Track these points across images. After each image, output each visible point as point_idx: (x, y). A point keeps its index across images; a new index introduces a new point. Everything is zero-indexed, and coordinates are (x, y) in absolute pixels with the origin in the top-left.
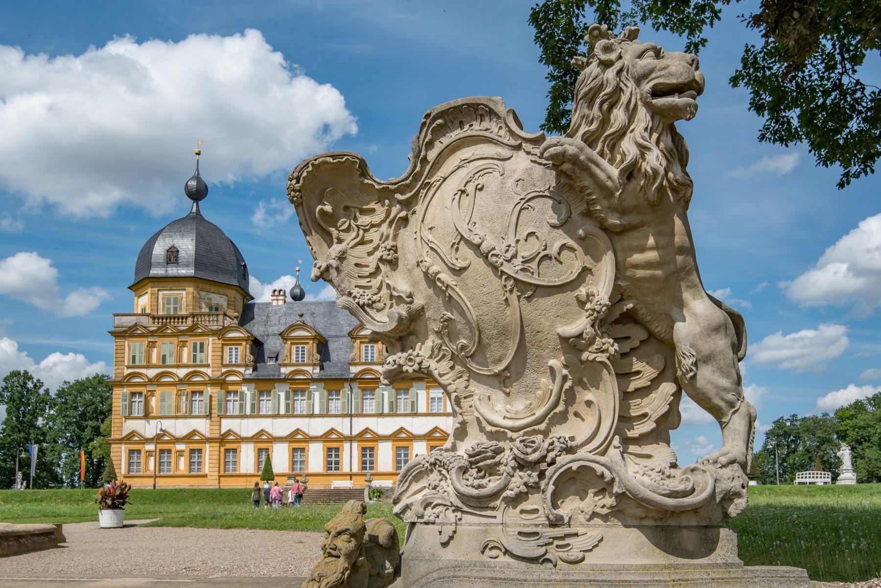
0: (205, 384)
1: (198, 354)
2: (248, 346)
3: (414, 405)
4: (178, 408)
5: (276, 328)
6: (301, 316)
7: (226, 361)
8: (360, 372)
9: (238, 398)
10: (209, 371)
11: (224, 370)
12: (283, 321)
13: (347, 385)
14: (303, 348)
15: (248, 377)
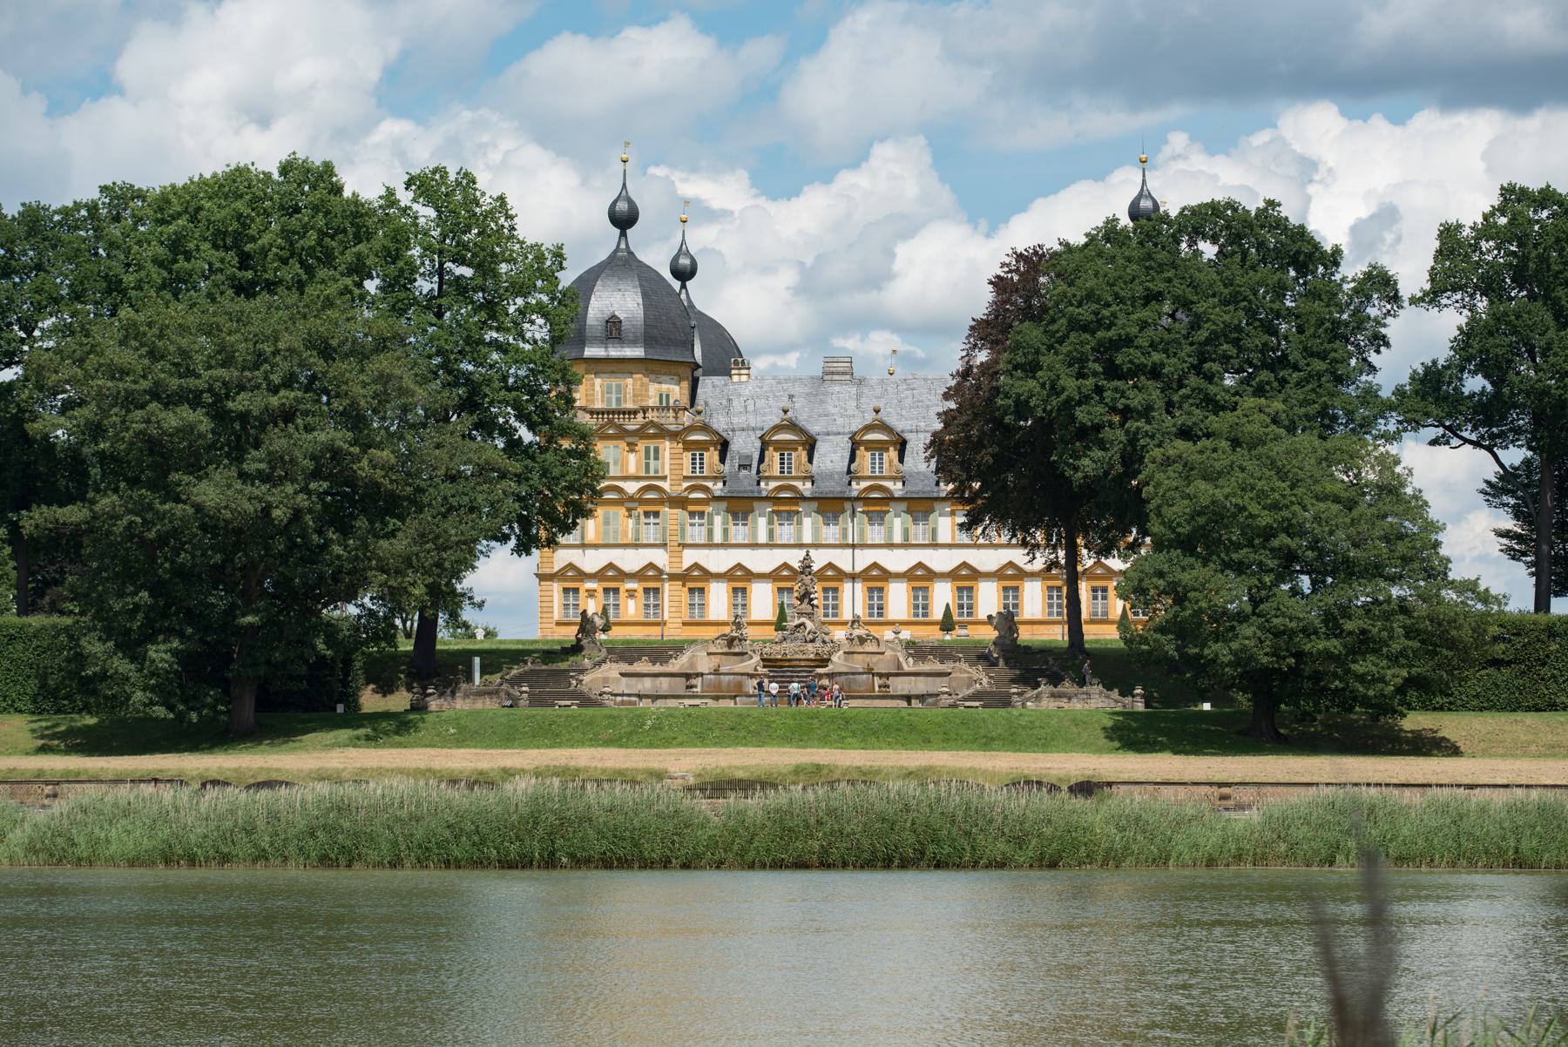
0: (661, 502)
1: (652, 462)
2: (716, 454)
3: (934, 531)
4: (625, 533)
5: (744, 418)
6: (785, 412)
7: (687, 472)
8: (866, 489)
9: (705, 521)
10: (666, 485)
11: (686, 485)
12: (751, 408)
13: (848, 505)
14: (790, 455)
15: (717, 493)
